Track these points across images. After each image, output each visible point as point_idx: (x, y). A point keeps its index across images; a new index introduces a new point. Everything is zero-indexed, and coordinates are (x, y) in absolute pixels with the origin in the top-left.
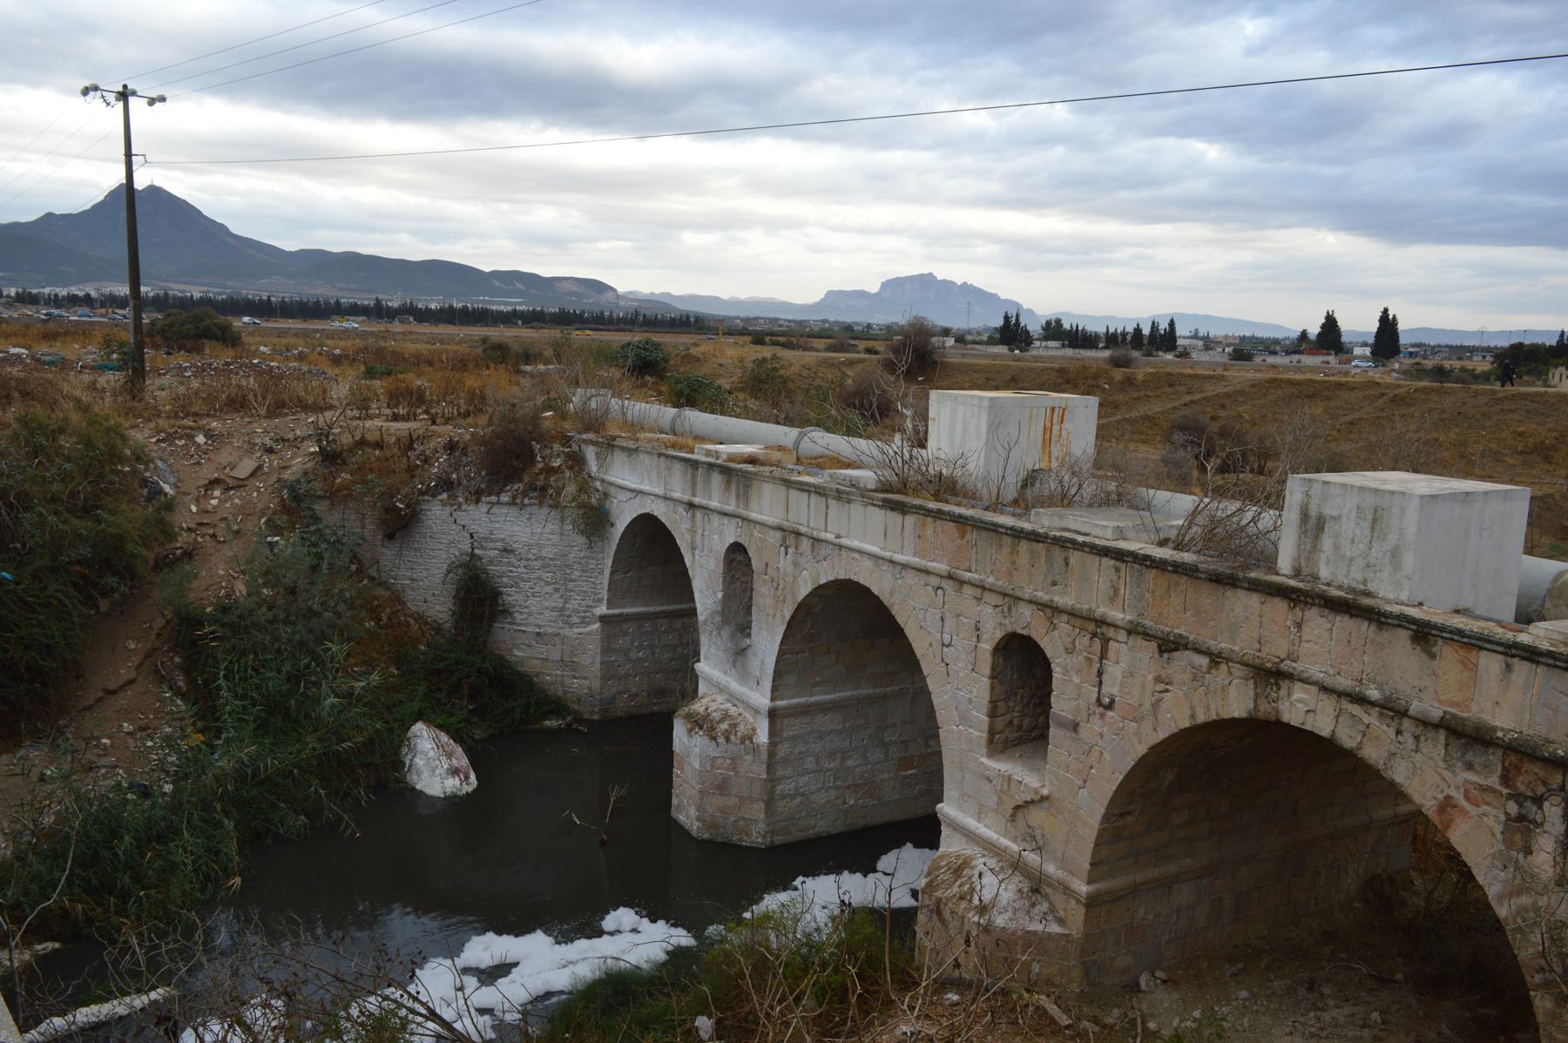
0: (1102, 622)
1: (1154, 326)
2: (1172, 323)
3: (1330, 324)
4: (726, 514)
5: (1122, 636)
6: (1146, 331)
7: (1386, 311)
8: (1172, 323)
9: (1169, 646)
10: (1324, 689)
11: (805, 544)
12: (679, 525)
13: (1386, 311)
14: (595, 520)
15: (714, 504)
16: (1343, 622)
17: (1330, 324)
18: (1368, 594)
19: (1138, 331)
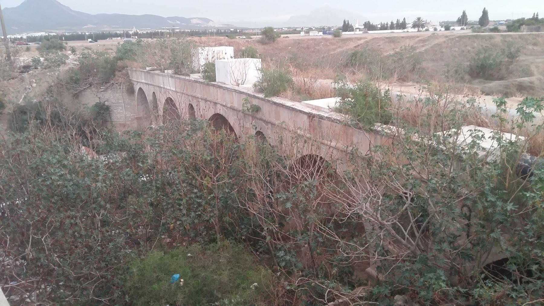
0: (198, 98)
1: (398, 21)
2: (404, 19)
3: (464, 15)
4: (151, 85)
5: (200, 100)
6: (395, 22)
7: (485, 8)
8: (404, 19)
9: (206, 101)
10: (221, 105)
11: (162, 88)
12: (145, 88)
13: (485, 8)
14: (131, 91)
15: (149, 82)
16: (222, 90)
17: (464, 15)
18: (225, 84)
19: (392, 23)
